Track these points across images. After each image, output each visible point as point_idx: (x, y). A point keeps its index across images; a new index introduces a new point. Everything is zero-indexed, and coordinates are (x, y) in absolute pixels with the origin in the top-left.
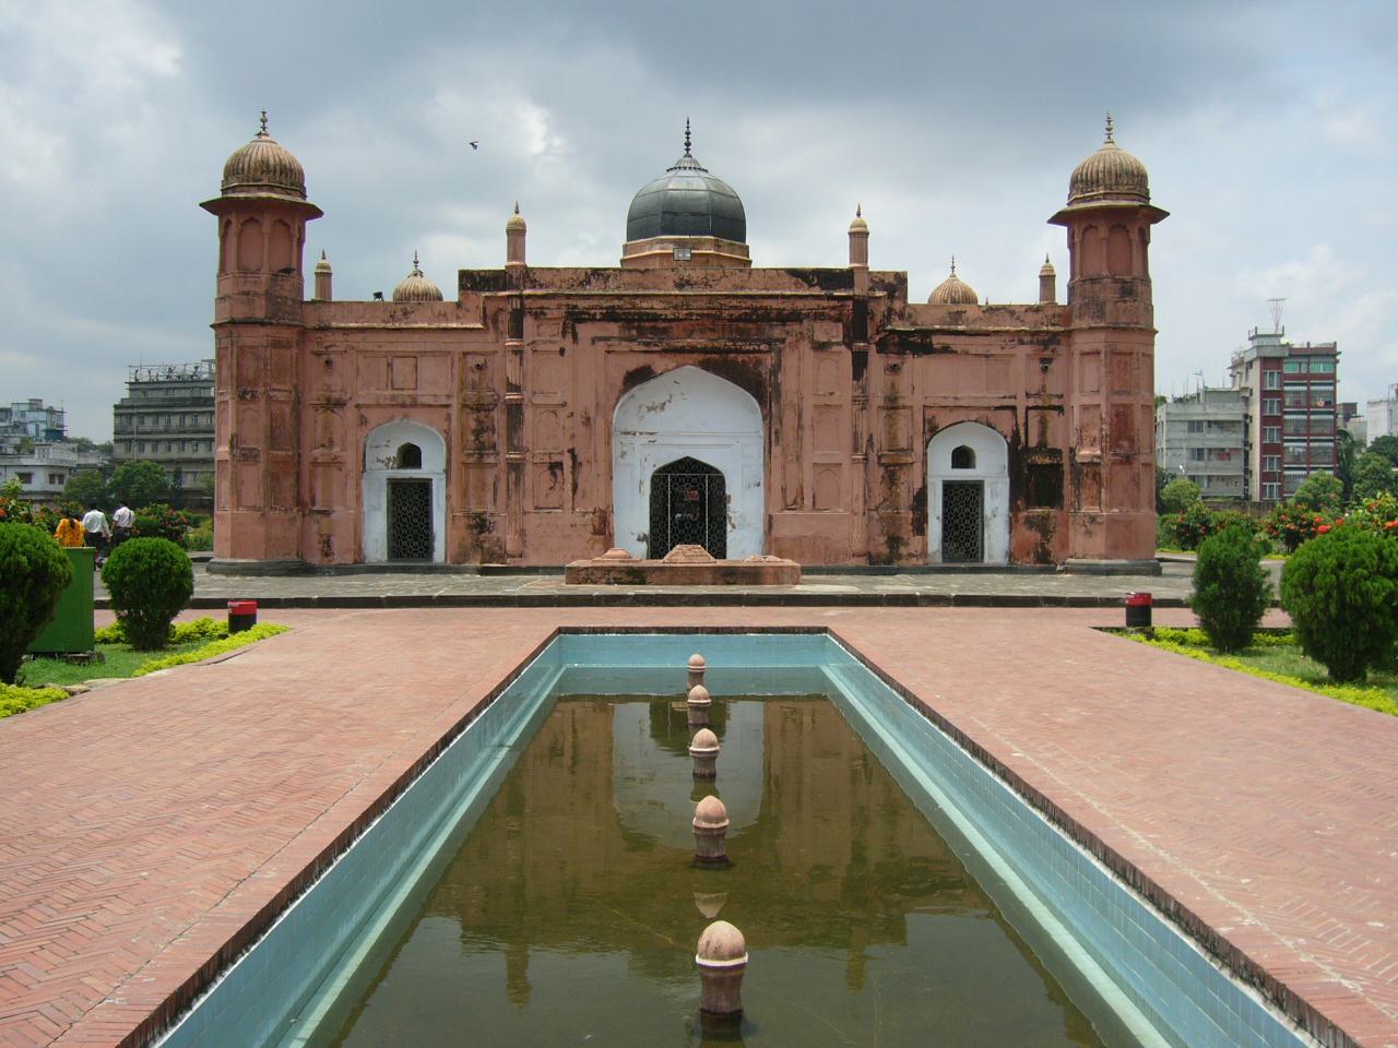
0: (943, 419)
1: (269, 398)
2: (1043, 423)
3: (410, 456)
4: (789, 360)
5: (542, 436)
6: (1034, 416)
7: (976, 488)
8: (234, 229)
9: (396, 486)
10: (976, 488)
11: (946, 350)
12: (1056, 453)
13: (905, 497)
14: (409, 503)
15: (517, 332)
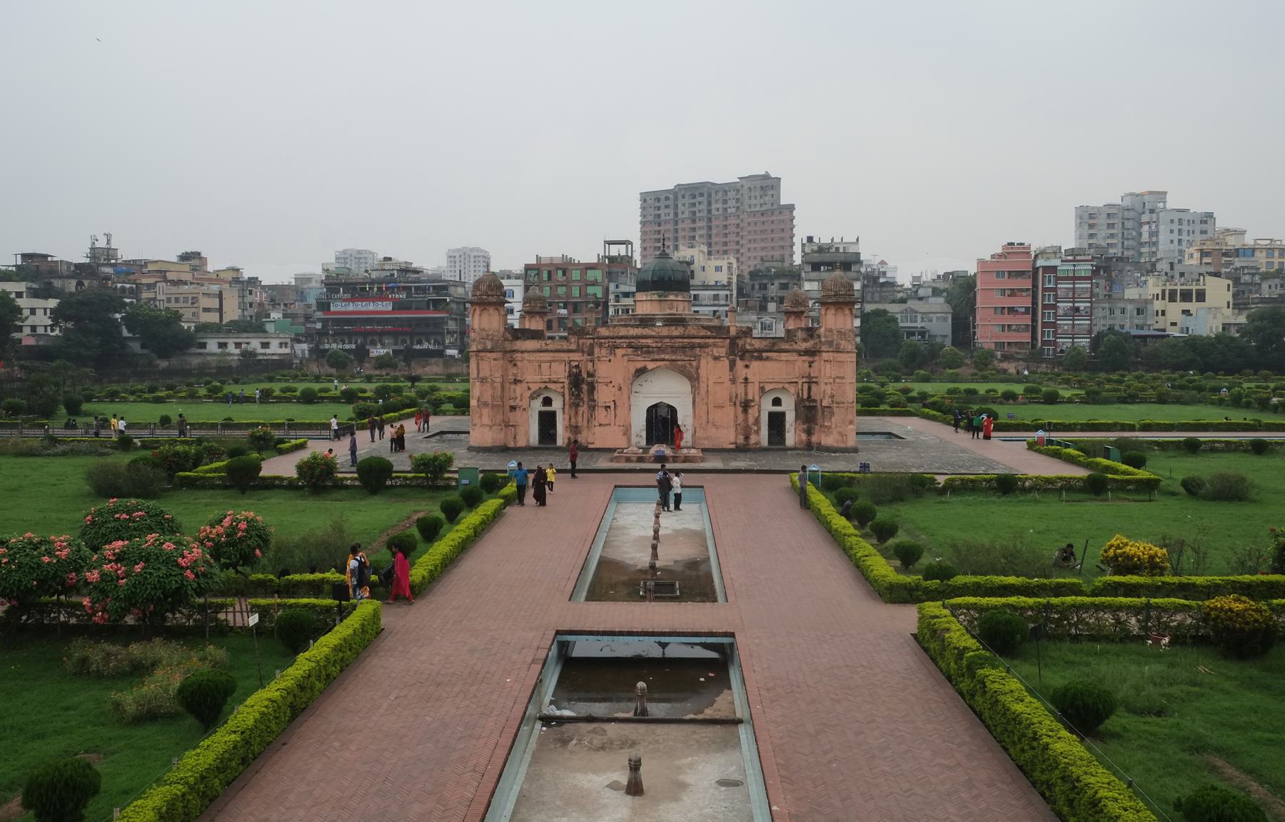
0: (768, 387)
1: (493, 382)
2: (809, 389)
3: (547, 401)
4: (703, 362)
5: (604, 395)
6: (806, 386)
7: (783, 414)
8: (478, 312)
9: (541, 413)
10: (783, 414)
11: (767, 359)
12: (815, 401)
13: (751, 420)
14: (547, 421)
15: (591, 353)
